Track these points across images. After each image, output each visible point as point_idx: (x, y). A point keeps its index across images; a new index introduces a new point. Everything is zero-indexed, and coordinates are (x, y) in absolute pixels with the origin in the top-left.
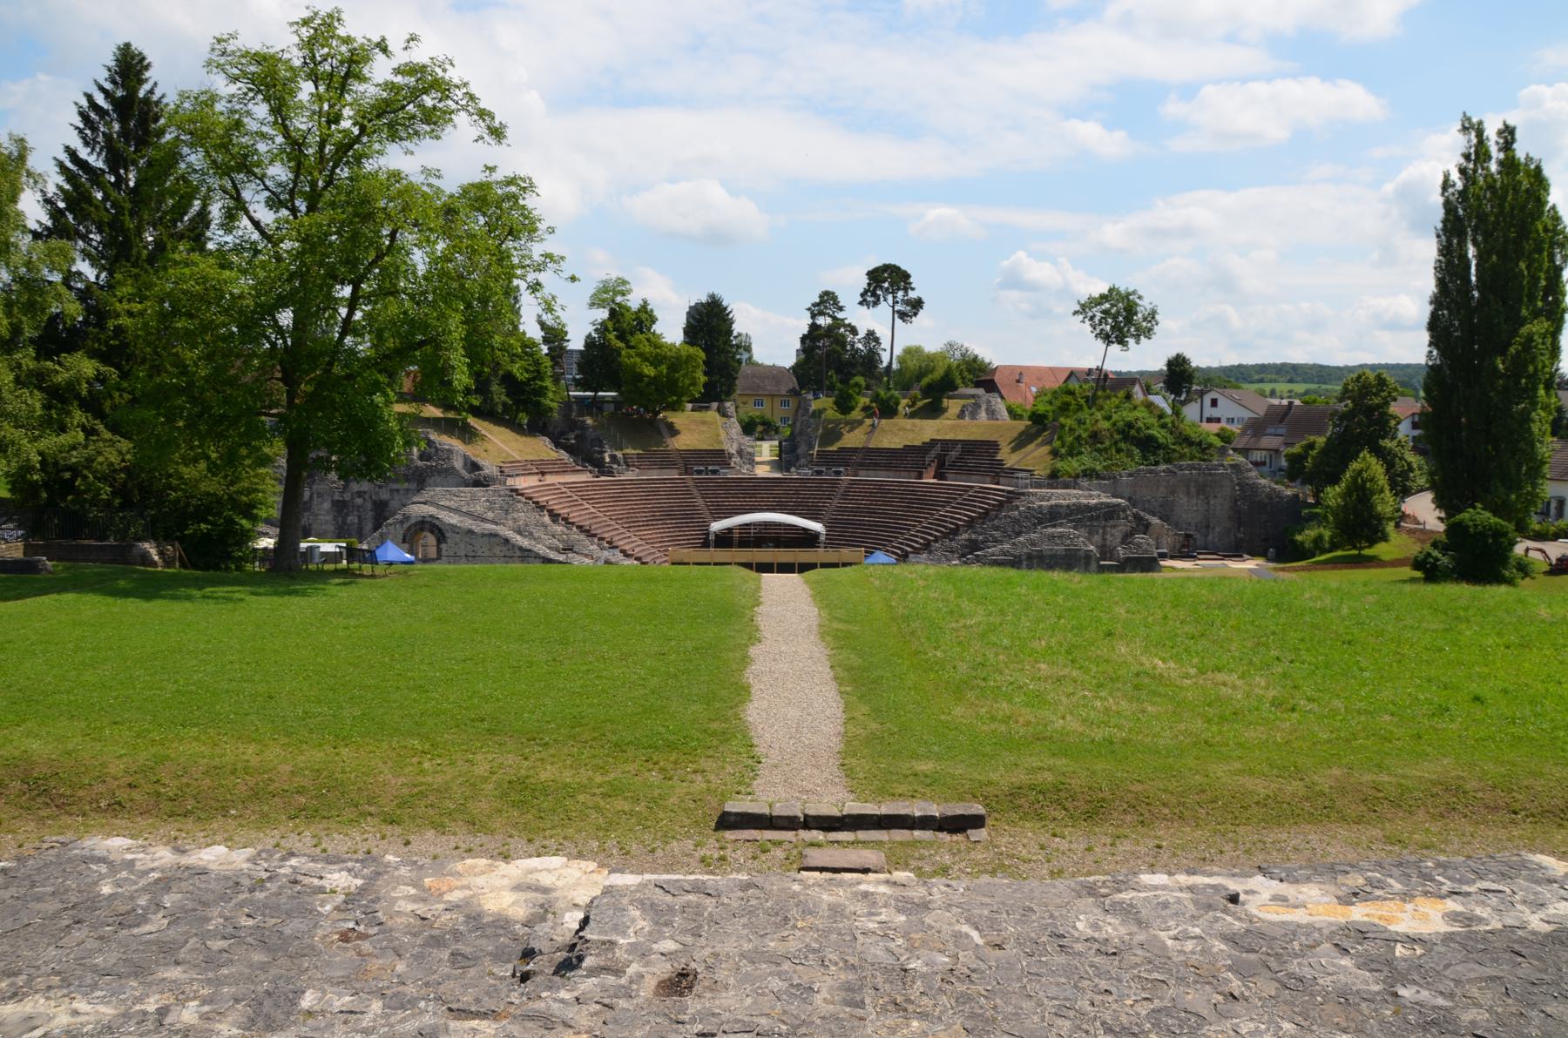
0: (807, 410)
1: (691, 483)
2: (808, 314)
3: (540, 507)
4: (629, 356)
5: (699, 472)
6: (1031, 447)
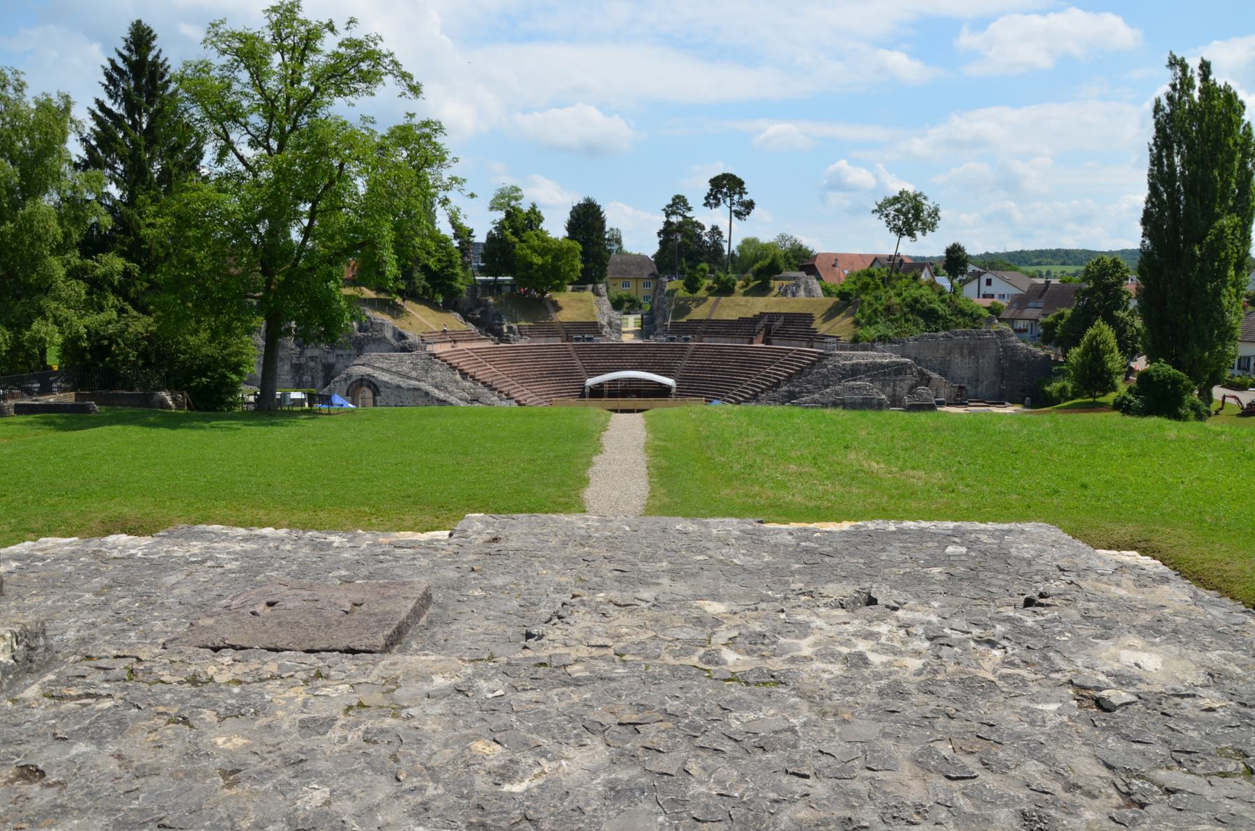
1: (571, 348)
2: (663, 214)
3: (453, 367)
4: (522, 249)
5: (578, 340)
6: (838, 318)
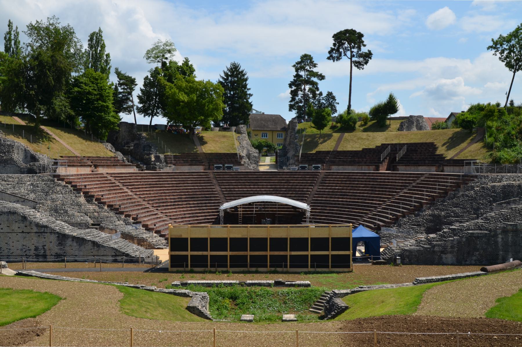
0: (294, 129)
1: (211, 175)
2: (294, 69)
3: (77, 190)
4: (171, 88)
5: (219, 168)
6: (463, 145)
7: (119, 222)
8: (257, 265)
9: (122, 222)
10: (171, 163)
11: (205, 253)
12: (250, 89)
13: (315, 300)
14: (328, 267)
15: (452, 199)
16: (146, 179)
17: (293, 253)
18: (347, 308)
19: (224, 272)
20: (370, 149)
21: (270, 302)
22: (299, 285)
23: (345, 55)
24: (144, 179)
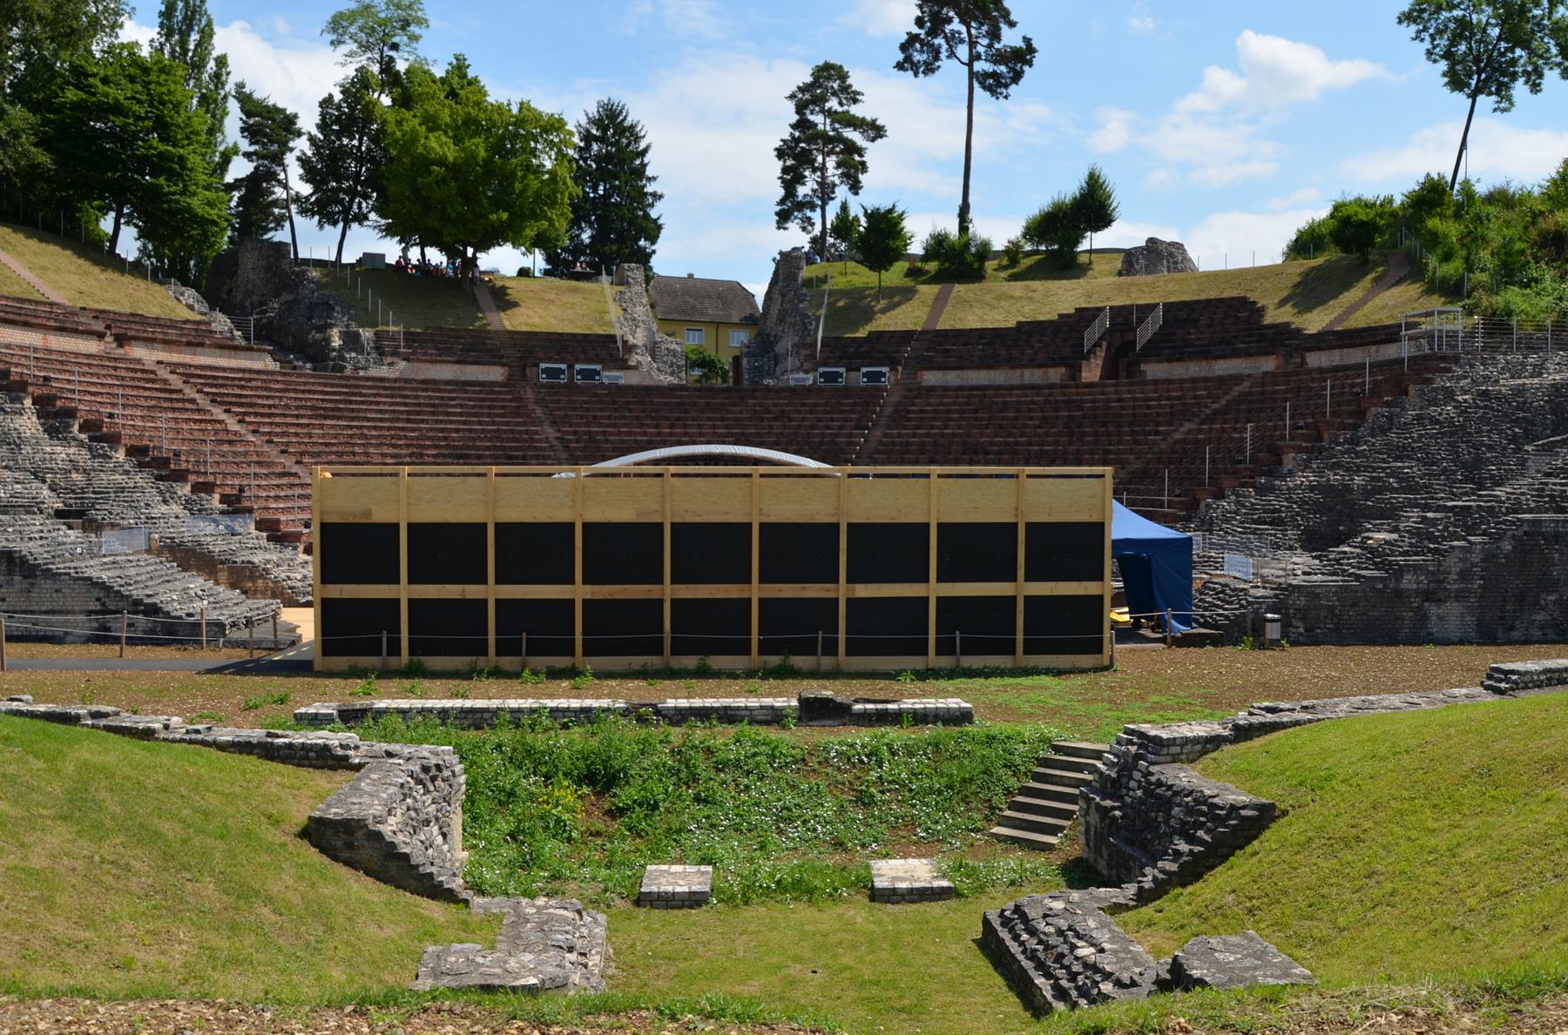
2: (791, 106)
7: (164, 508)
8: (709, 638)
9: (176, 508)
10: (395, 354)
11: (473, 591)
12: (654, 178)
13: (1013, 783)
14: (1012, 652)
15: (1384, 432)
16: (303, 392)
17: (865, 591)
18: (1266, 815)
19: (554, 674)
20: (1040, 323)
21: (789, 798)
22: (921, 718)
23: (952, 55)
24: (296, 391)
